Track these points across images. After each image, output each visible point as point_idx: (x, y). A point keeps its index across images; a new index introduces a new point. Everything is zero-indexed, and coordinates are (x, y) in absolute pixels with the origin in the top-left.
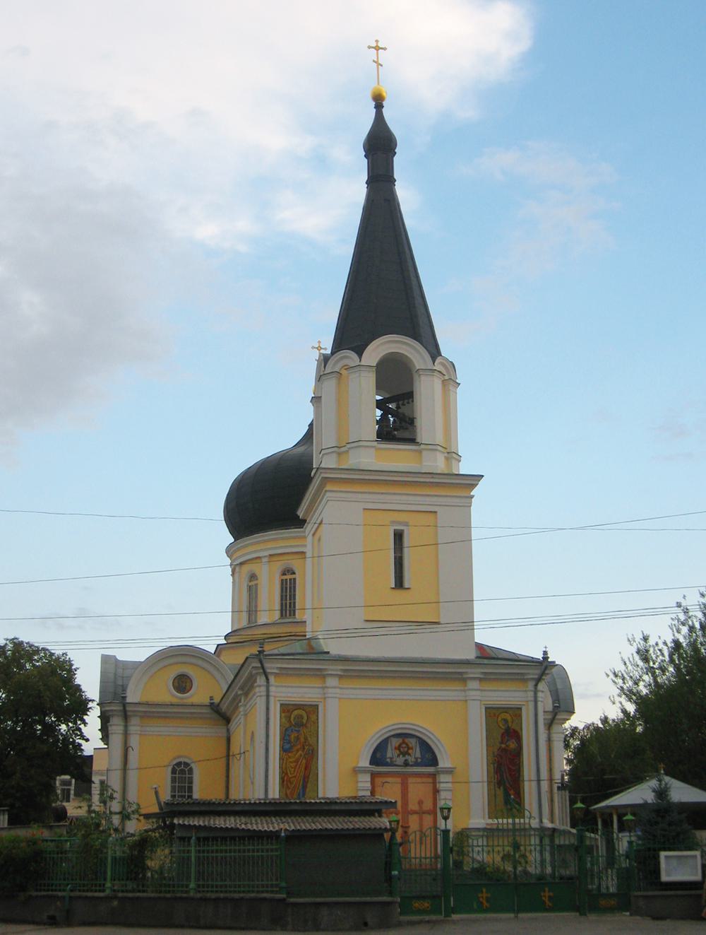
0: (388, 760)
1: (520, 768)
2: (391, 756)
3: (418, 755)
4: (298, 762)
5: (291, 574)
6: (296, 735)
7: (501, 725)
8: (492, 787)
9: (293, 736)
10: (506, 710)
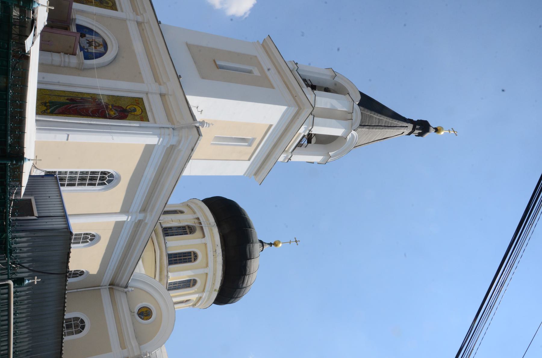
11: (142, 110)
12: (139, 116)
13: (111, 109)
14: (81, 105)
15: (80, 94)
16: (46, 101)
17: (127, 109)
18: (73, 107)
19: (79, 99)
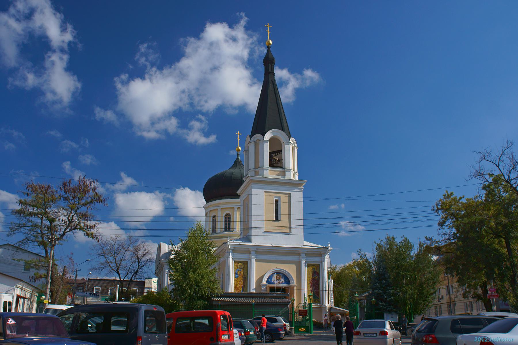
0: (273, 282)
1: (319, 285)
5: (229, 215)
6: (240, 272)
9: (239, 273)
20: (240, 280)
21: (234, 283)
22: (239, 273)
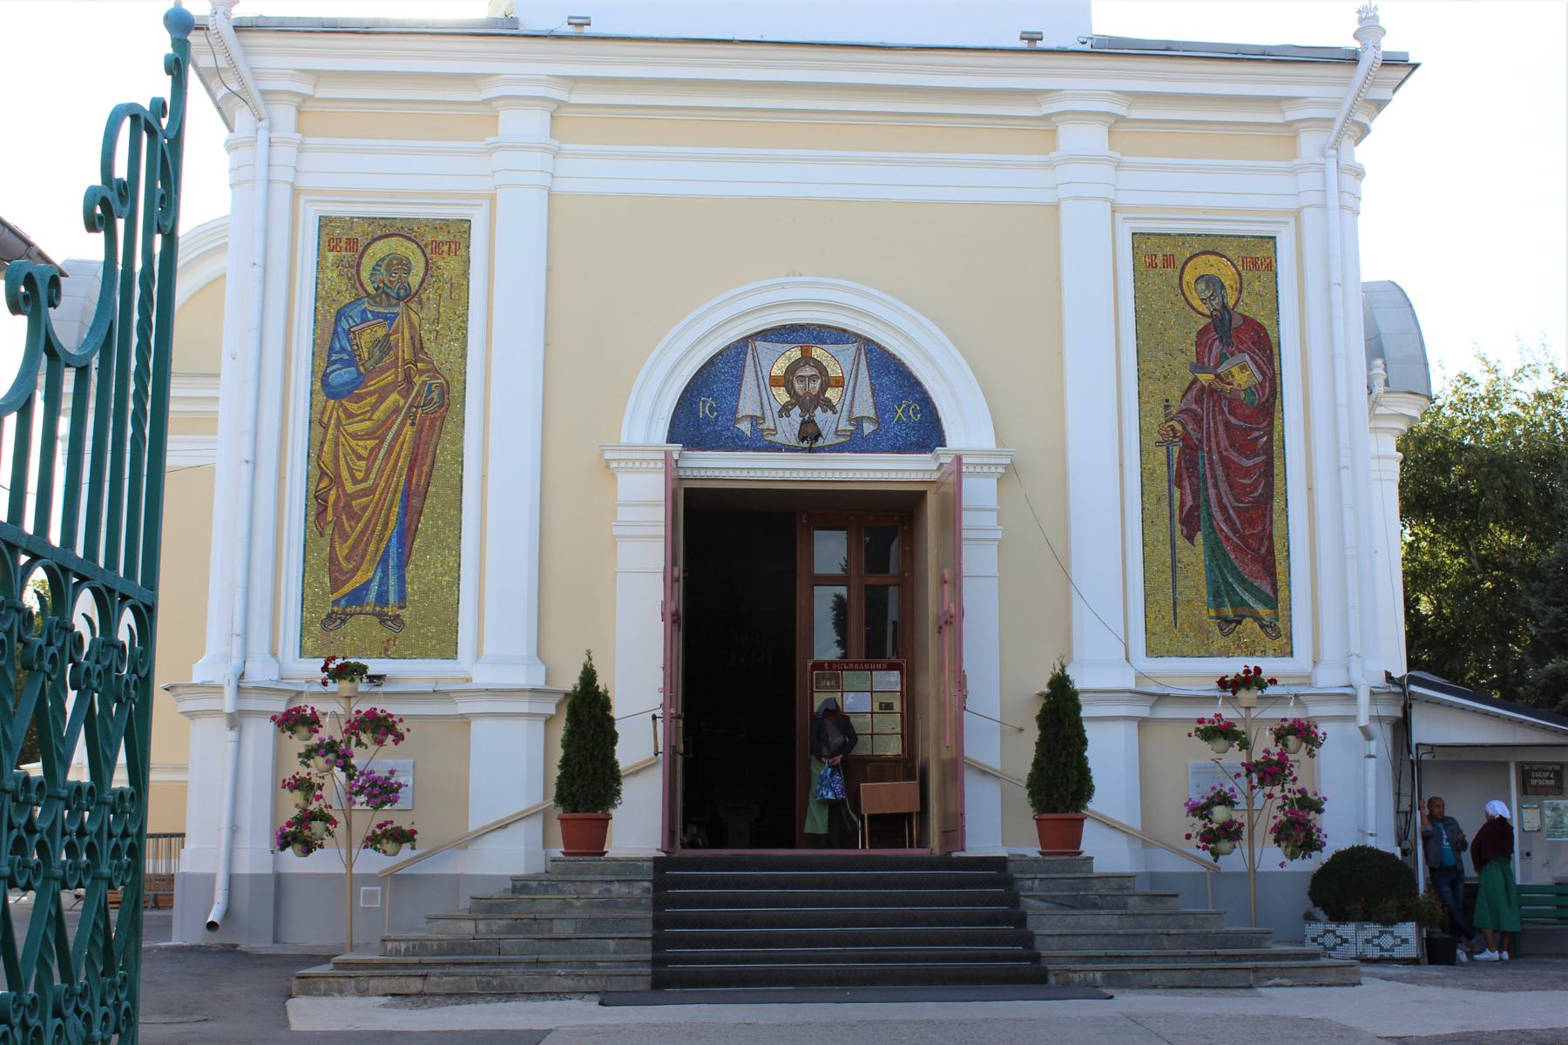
0: (745, 427)
2: (759, 414)
3: (865, 406)
4: (382, 439)
6: (381, 333)
7: (1197, 303)
8: (1164, 537)
9: (366, 339)
10: (1211, 246)
11: (1204, 253)
12: (1244, 273)
13: (1218, 376)
14: (1212, 491)
15: (1147, 488)
16: (1211, 617)
17: (1207, 312)
18: (1228, 520)
19: (1181, 494)
20: (379, 414)
21: (315, 454)
22: (366, 339)
